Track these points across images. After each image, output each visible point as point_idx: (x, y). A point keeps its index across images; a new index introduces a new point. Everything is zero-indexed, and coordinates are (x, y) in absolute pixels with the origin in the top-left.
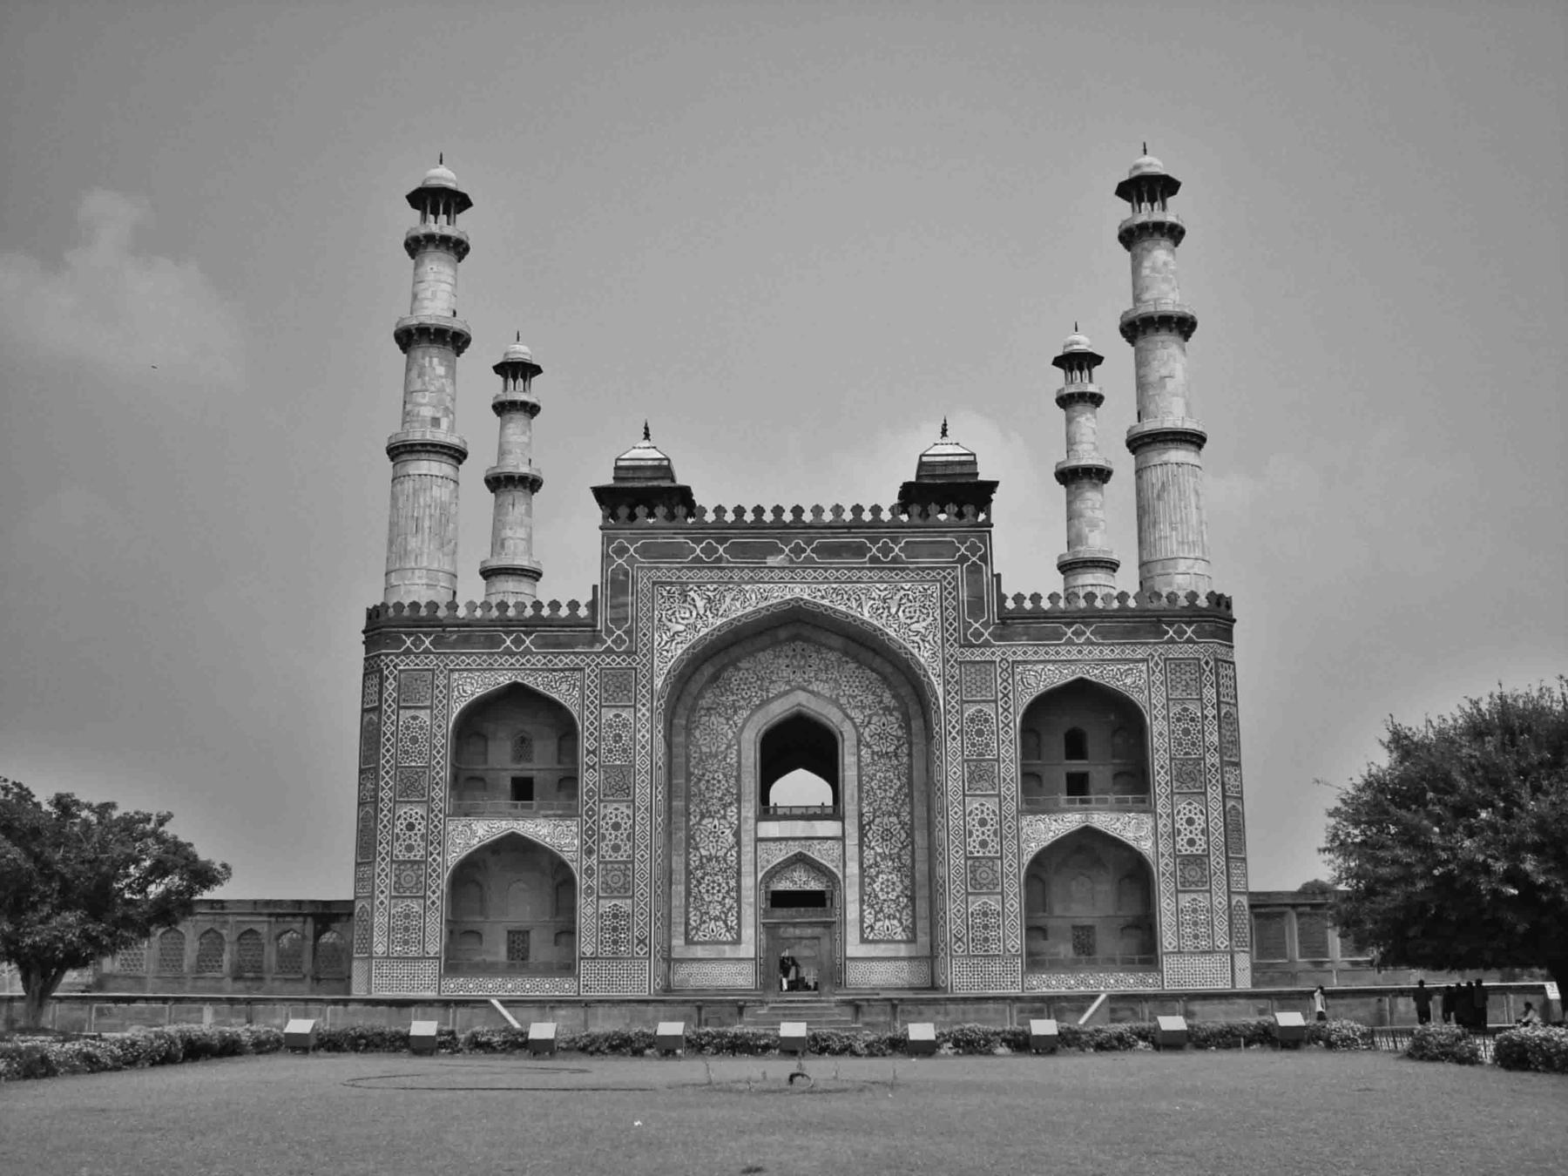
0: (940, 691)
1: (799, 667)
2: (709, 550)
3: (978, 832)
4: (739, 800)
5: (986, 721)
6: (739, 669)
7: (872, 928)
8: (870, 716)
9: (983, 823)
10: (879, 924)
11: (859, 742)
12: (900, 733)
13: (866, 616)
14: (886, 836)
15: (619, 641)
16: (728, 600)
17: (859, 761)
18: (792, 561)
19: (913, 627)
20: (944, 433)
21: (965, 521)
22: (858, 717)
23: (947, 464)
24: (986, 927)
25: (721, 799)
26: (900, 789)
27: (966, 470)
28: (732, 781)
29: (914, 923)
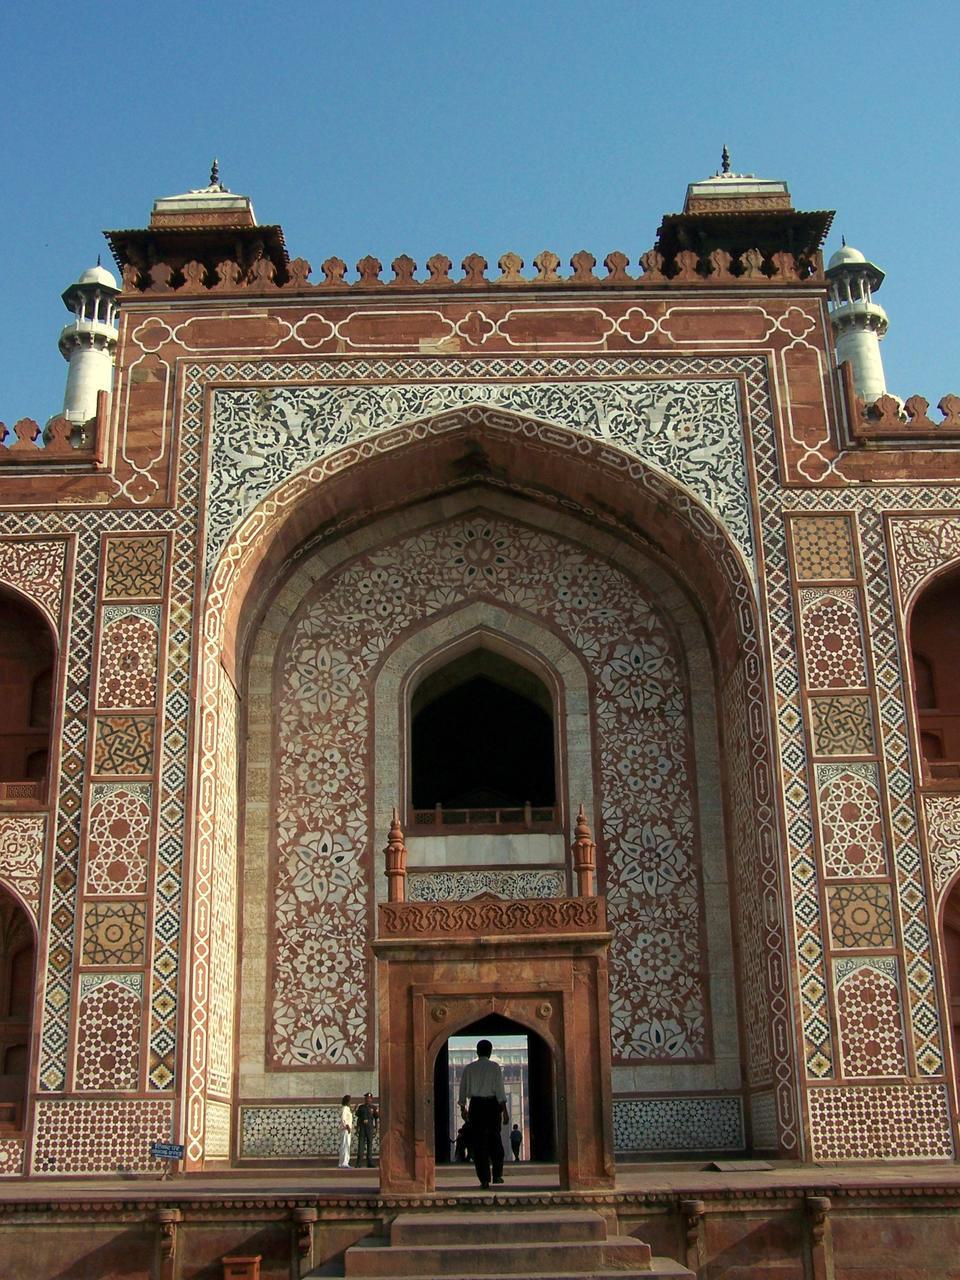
0: (749, 565)
1: (480, 562)
2: (313, 332)
3: (841, 830)
4: (370, 799)
5: (844, 620)
6: (372, 568)
7: (628, 1038)
8: (612, 646)
9: (851, 813)
10: (639, 1029)
11: (593, 691)
12: (668, 675)
13: (606, 436)
14: (649, 859)
15: (141, 487)
16: (346, 413)
17: (594, 725)
18: (465, 346)
19: (698, 454)
20: (725, 166)
21: (777, 279)
22: (591, 648)
23: (735, 198)
24: (871, 1022)
25: (336, 797)
26: (672, 773)
27: (772, 205)
28: (358, 765)
29: (708, 1025)
